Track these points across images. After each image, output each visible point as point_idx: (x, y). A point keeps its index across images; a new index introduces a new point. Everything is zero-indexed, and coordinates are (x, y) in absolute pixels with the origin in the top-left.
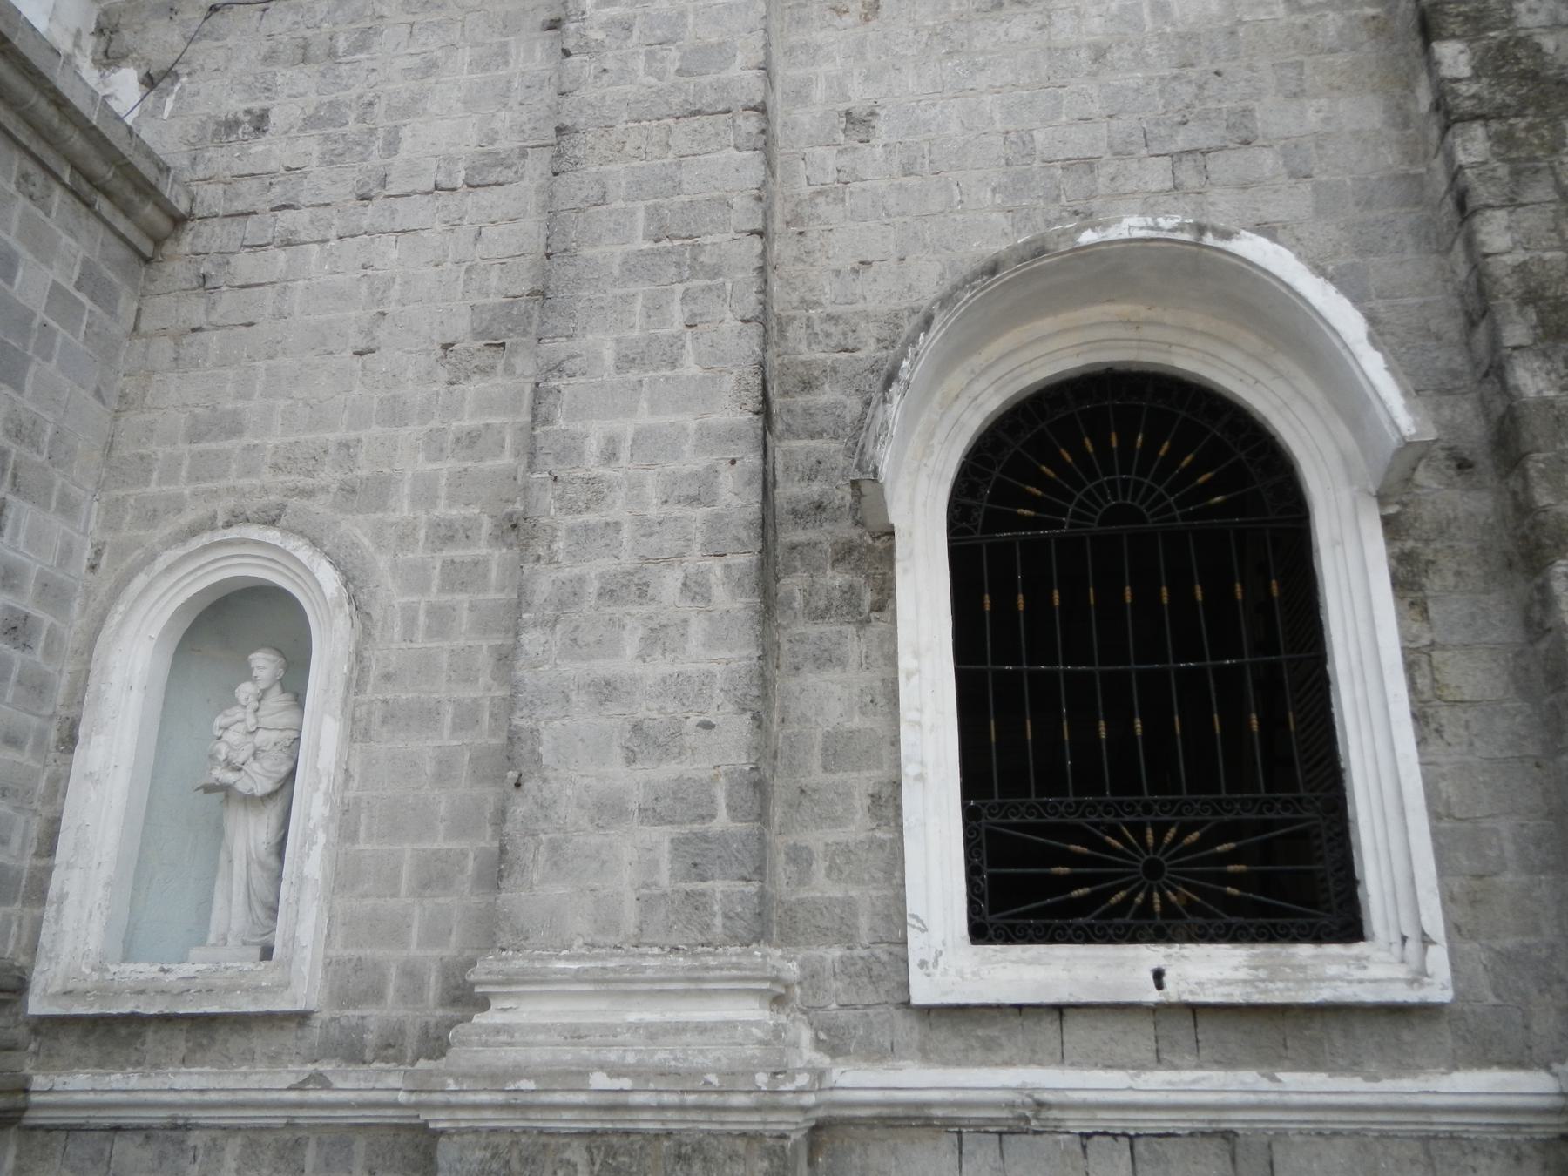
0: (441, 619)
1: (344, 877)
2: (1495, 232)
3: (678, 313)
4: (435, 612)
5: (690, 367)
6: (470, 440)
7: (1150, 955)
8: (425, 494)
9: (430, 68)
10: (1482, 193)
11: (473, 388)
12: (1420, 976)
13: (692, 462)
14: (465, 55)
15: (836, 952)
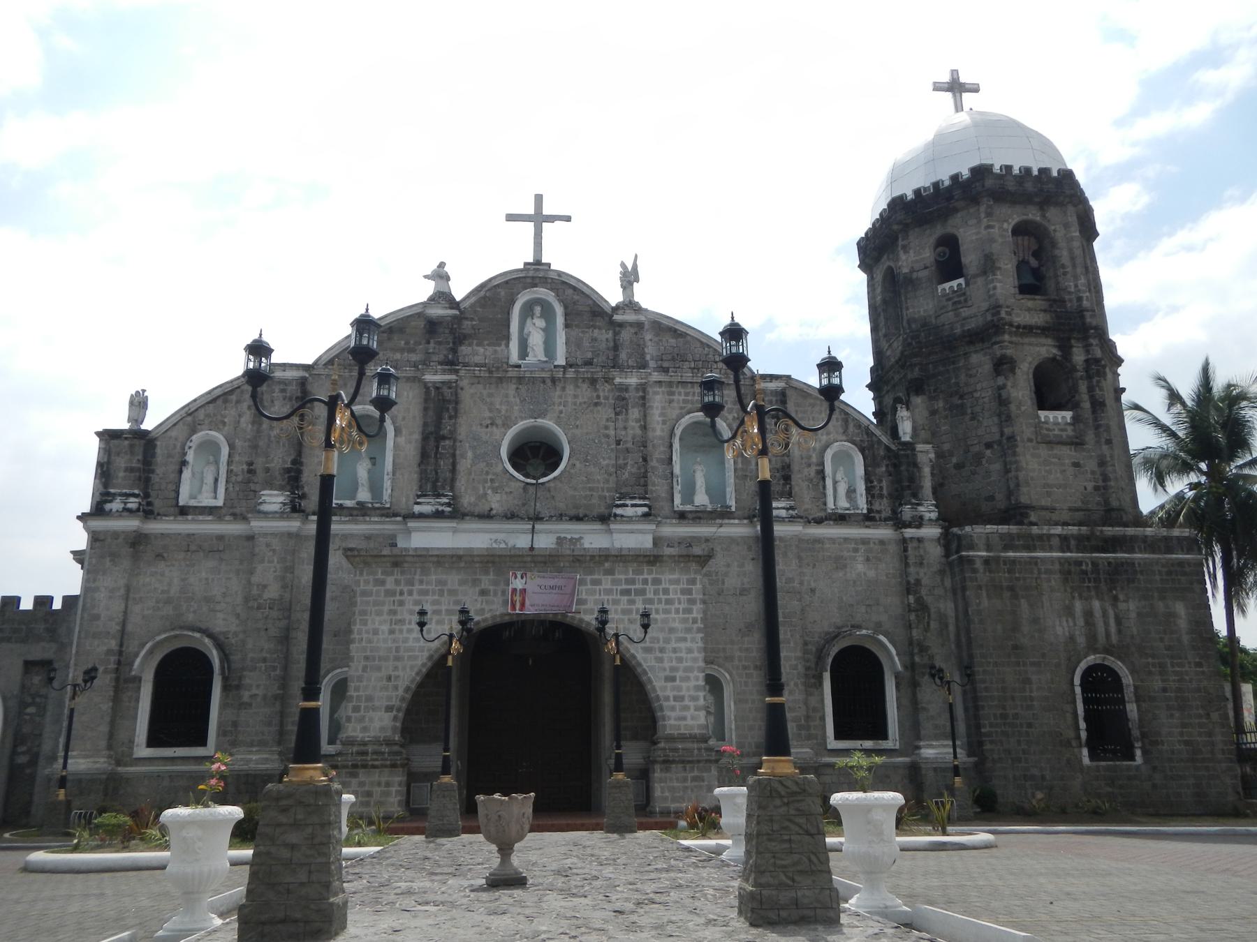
0: (746, 684)
1: (737, 728)
2: (915, 633)
3: (789, 634)
4: (745, 682)
5: (792, 645)
6: (747, 650)
7: (860, 742)
8: (740, 660)
9: (728, 566)
10: (913, 626)
11: (746, 639)
12: (895, 745)
13: (794, 662)
14: (736, 564)
15: (815, 741)
